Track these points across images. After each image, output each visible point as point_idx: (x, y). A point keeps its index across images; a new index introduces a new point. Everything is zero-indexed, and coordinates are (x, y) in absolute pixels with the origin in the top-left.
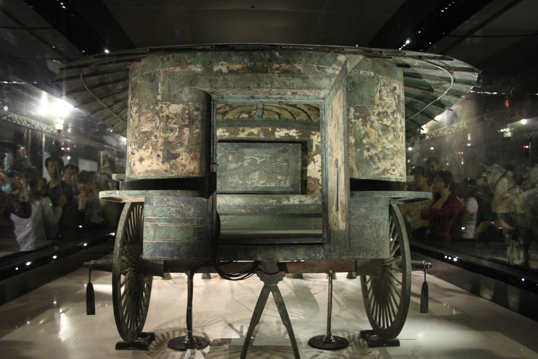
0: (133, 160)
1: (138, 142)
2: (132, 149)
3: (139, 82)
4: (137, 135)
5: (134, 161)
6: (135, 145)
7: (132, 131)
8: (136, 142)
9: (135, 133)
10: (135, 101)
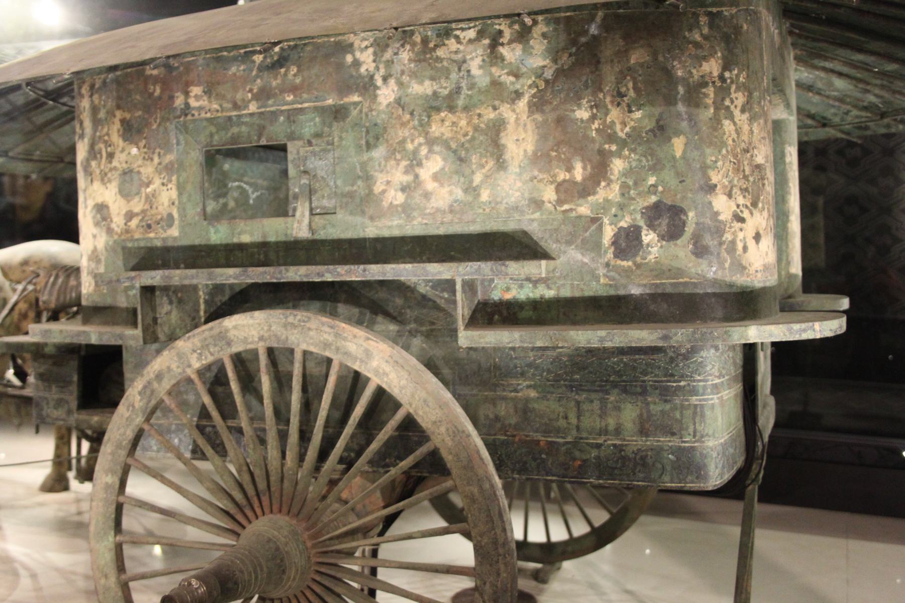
0: (741, 235)
1: (750, 190)
2: (738, 206)
3: (745, 27)
4: (748, 171)
5: (744, 238)
6: (744, 197)
7: (735, 156)
8: (746, 190)
9: (744, 165)
10: (738, 76)
